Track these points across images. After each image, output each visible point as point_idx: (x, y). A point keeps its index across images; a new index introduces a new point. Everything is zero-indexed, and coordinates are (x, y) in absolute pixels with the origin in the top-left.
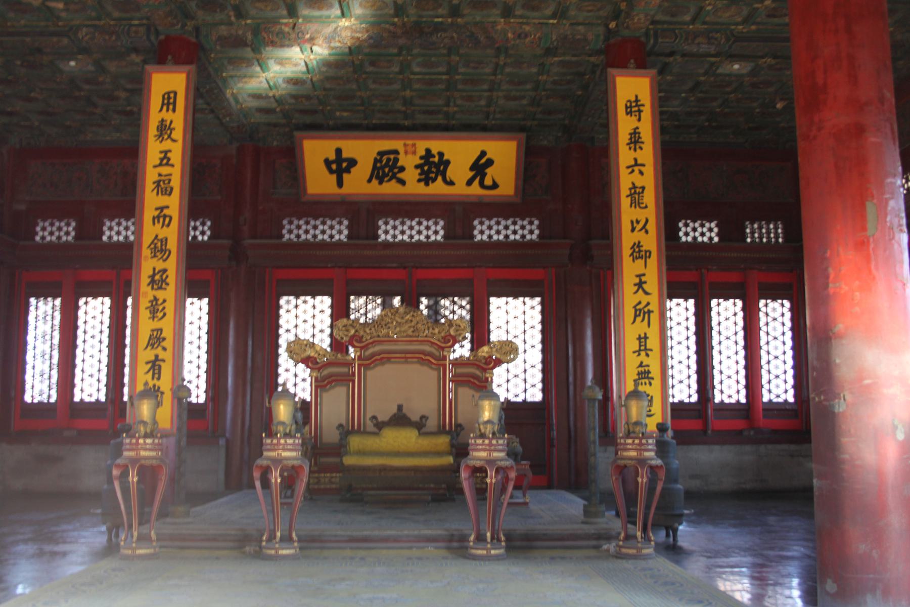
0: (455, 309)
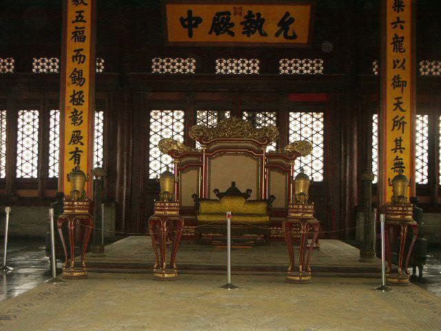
0: (267, 120)
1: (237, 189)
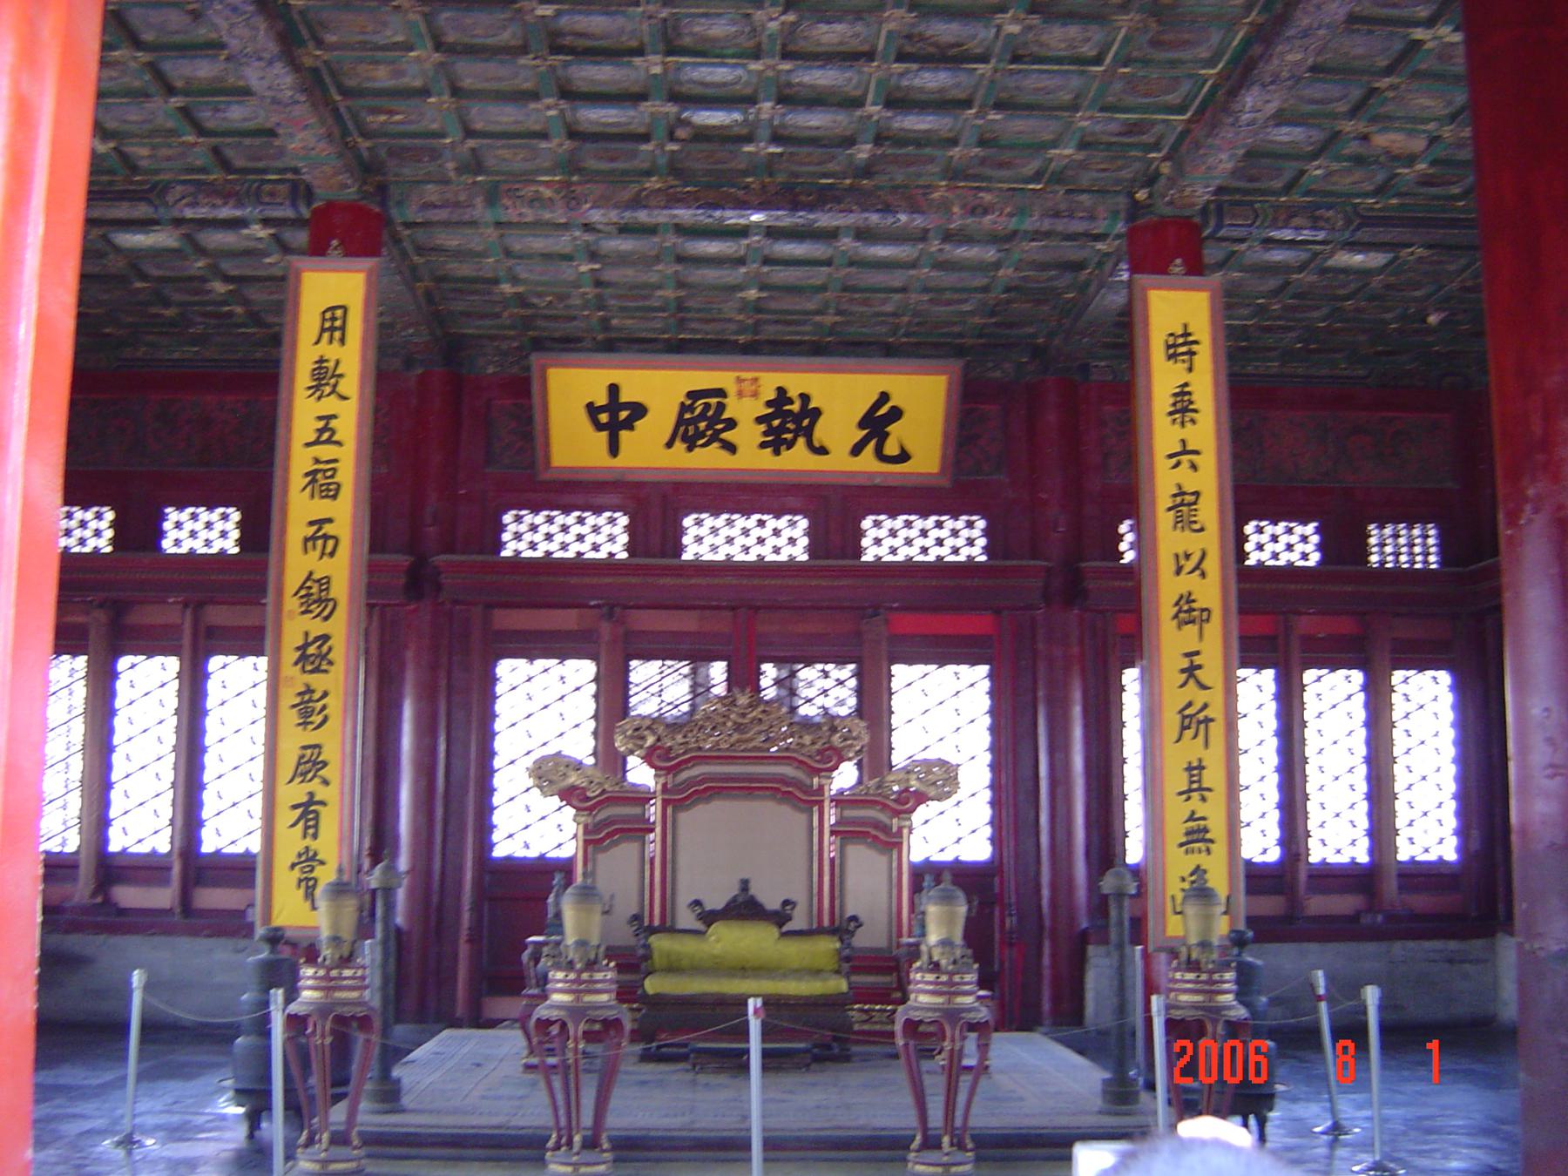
0: (827, 689)
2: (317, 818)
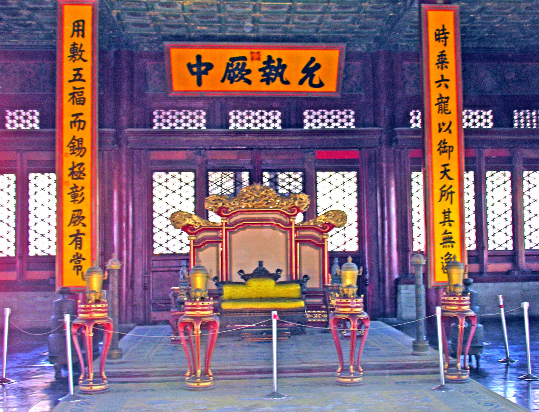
0: (291, 182)
1: (264, 268)
2: (81, 241)
